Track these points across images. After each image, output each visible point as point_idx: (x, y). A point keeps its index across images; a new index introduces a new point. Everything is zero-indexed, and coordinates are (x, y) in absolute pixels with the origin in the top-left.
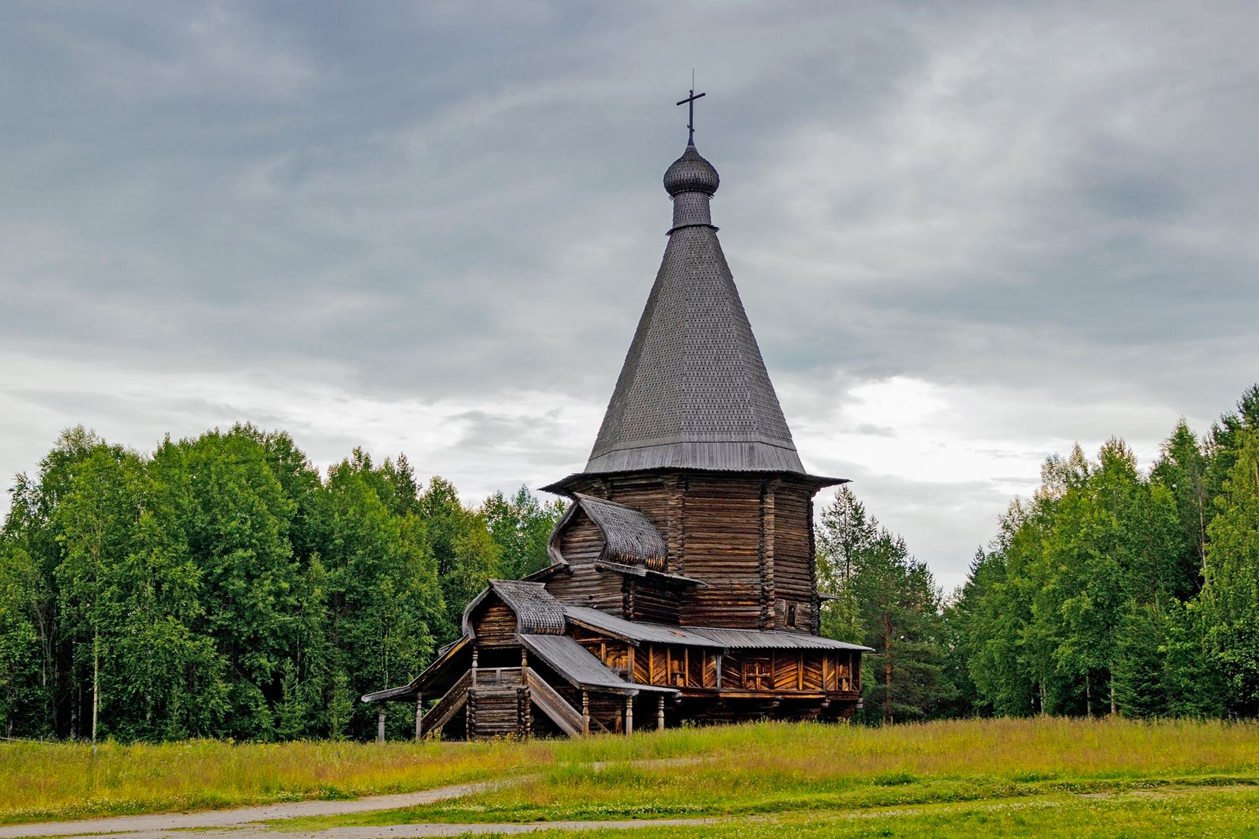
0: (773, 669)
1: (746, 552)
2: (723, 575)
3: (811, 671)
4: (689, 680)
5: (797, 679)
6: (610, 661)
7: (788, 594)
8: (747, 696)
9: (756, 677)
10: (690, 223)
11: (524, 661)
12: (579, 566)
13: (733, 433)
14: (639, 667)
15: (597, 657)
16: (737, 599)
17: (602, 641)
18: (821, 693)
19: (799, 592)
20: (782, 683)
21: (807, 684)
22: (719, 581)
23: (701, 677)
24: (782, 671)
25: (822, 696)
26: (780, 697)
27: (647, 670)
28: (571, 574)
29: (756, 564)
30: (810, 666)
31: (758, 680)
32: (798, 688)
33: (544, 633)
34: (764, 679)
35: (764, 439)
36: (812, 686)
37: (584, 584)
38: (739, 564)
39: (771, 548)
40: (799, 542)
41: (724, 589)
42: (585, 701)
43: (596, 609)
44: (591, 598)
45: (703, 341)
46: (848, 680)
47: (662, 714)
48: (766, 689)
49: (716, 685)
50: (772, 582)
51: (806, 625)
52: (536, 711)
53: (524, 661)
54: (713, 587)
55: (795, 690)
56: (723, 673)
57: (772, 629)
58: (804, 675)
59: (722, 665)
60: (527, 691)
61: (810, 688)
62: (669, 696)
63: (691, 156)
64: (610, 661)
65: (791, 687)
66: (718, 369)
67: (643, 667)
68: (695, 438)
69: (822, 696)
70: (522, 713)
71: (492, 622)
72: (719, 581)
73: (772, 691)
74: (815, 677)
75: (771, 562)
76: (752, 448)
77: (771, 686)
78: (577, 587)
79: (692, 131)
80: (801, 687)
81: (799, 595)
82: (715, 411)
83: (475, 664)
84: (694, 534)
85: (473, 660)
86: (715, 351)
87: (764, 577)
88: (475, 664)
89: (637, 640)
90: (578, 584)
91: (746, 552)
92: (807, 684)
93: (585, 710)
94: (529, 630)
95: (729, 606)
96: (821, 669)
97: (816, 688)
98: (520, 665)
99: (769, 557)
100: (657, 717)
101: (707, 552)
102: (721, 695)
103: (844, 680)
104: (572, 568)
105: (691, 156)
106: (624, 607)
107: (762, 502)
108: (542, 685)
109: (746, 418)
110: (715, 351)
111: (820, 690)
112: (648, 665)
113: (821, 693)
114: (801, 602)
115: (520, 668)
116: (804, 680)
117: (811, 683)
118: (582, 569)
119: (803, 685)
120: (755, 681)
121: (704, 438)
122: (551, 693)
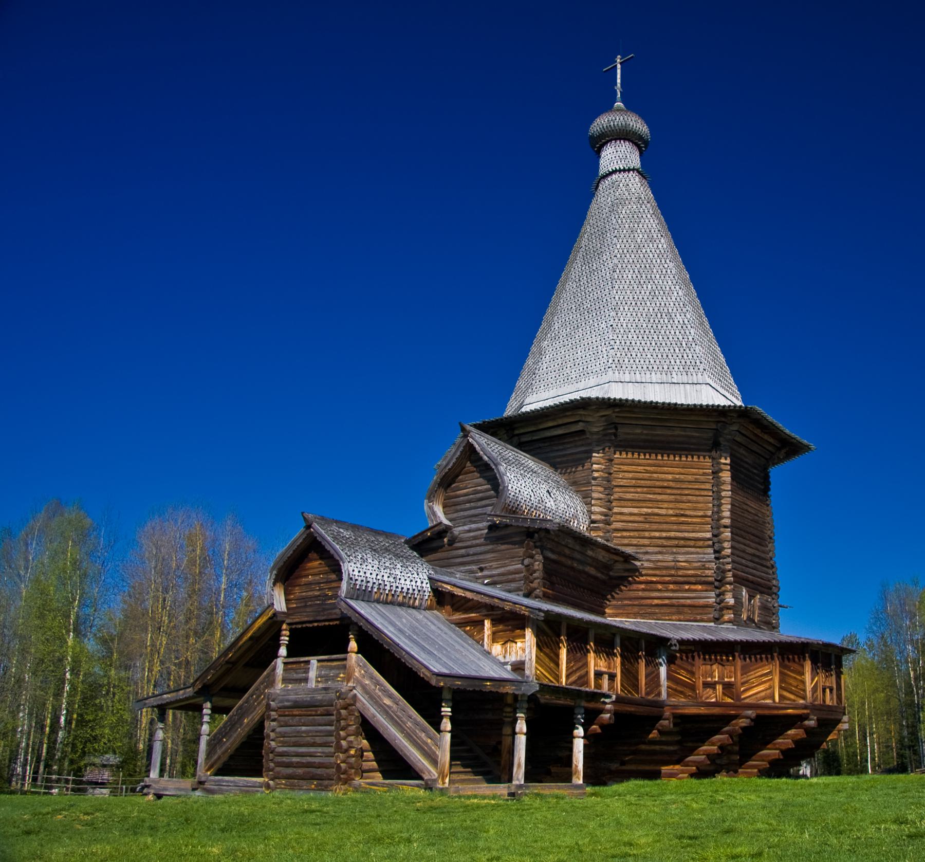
1: (695, 520)
2: (664, 550)
4: (622, 685)
9: (716, 683)
11: (353, 645)
12: (466, 528)
17: (487, 616)
20: (751, 693)
21: (786, 694)
22: (660, 557)
24: (752, 675)
25: (805, 711)
26: (749, 712)
29: (709, 535)
30: (788, 668)
31: (719, 688)
32: (774, 700)
34: (728, 687)
36: (792, 697)
37: (472, 551)
38: (686, 535)
39: (727, 514)
40: (757, 518)
41: (667, 568)
44: (481, 569)
45: (634, 276)
46: (831, 690)
50: (729, 560)
52: (369, 730)
53: (353, 645)
54: (651, 565)
55: (768, 701)
58: (781, 681)
61: (789, 699)
65: (764, 699)
66: (653, 305)
67: (551, 659)
71: (310, 584)
72: (660, 557)
73: (738, 703)
74: (795, 683)
75: (727, 534)
77: (737, 697)
78: (463, 556)
82: (651, 349)
90: (463, 551)
91: (695, 520)
92: (786, 694)
93: (447, 725)
95: (673, 591)
96: (803, 674)
99: (726, 527)
103: (828, 691)
104: (457, 531)
106: (526, 578)
109: (690, 357)
111: (802, 701)
112: (558, 656)
114: (761, 593)
116: (781, 688)
118: (469, 531)
119: (781, 696)
120: (715, 689)
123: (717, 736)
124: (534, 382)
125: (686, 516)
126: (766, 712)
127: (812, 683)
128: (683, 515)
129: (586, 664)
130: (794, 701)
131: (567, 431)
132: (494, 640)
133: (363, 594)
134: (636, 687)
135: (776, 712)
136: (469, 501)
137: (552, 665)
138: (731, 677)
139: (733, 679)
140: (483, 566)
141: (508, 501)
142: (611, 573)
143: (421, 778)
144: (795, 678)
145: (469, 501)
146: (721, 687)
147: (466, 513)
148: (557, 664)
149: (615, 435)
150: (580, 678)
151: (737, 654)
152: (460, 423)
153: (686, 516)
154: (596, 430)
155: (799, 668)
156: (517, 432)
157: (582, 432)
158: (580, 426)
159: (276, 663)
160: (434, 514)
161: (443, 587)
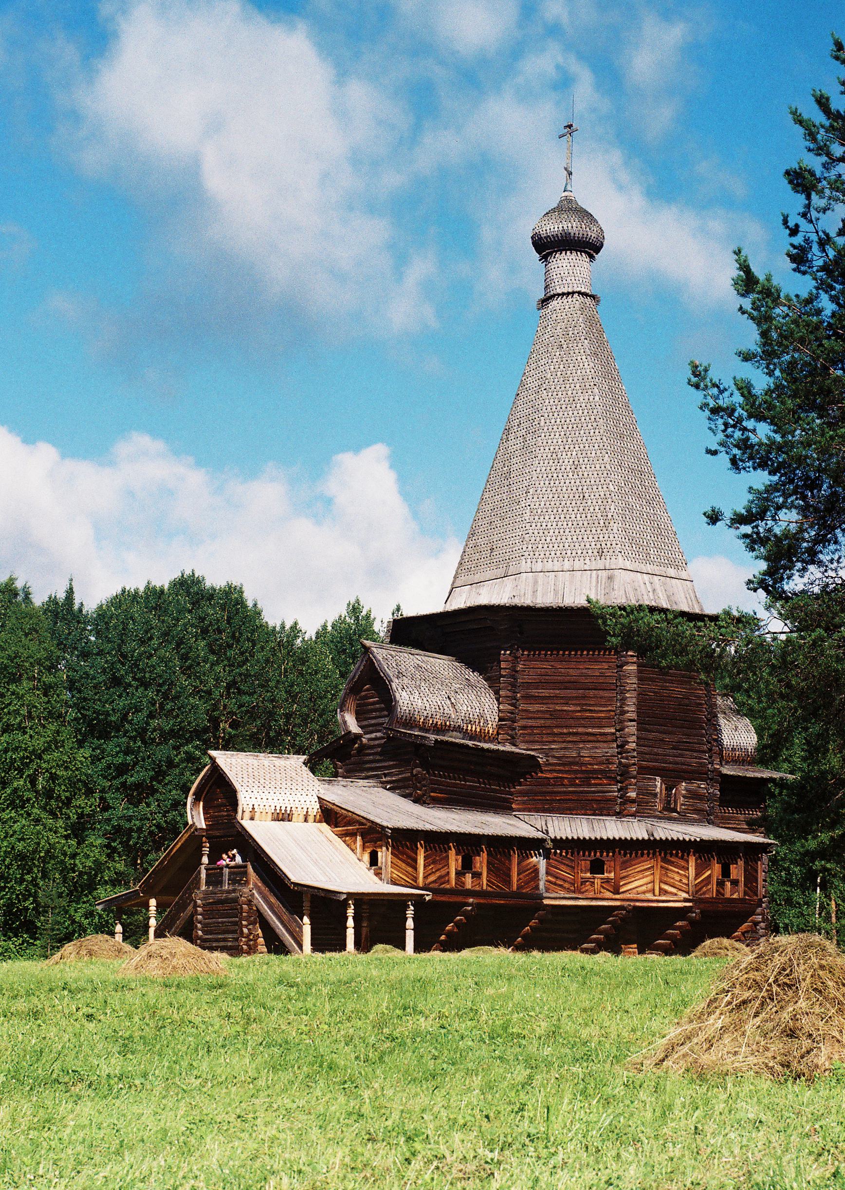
0: (618, 868)
3: (671, 870)
5: (653, 882)
7: (664, 769)
10: (559, 291)
13: (577, 559)
14: (400, 863)
15: (353, 850)
16: (588, 777)
18: (686, 900)
19: (684, 767)
22: (562, 753)
23: (509, 876)
24: (630, 871)
30: (672, 863)
35: (628, 565)
36: (674, 890)
43: (387, 790)
47: (410, 923)
49: (537, 887)
51: (697, 811)
55: (649, 896)
57: (633, 815)
59: (488, 862)
61: (671, 893)
62: (418, 901)
65: (644, 893)
67: (408, 864)
68: (539, 567)
69: (690, 904)
70: (244, 923)
72: (561, 753)
74: (677, 878)
75: (632, 728)
76: (610, 578)
79: (570, 174)
81: (684, 771)
84: (534, 692)
85: (203, 855)
86: (574, 453)
87: (621, 746)
88: (205, 860)
89: (388, 827)
96: (688, 869)
97: (680, 893)
100: (404, 929)
101: (547, 716)
102: (546, 902)
110: (574, 453)
112: (415, 861)
113: (686, 900)
116: (661, 881)
119: (660, 889)
121: (549, 566)
123: (603, 926)
125: (591, 711)
127: (696, 880)
128: (586, 711)
129: (447, 865)
134: (508, 881)
135: (638, 904)
136: (375, 710)
137: (410, 869)
138: (610, 872)
139: (612, 874)
144: (678, 873)
145: (375, 710)
147: (373, 722)
148: (415, 868)
150: (440, 877)
151: (617, 850)
153: (591, 711)
155: (683, 863)
160: (345, 722)
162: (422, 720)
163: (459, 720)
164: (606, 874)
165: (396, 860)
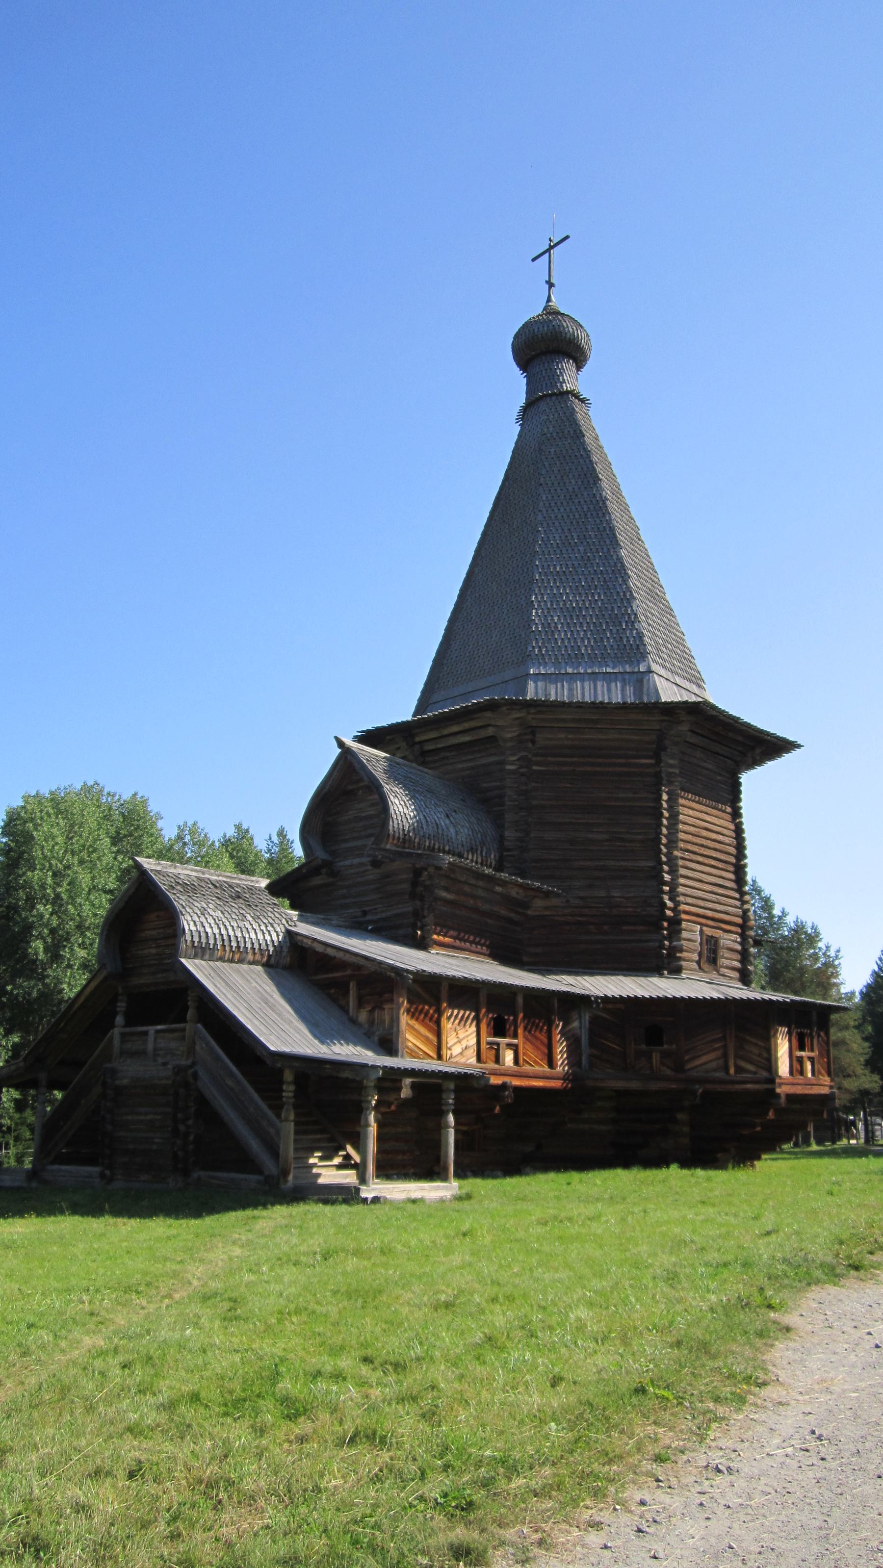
5: (725, 1056)
6: (363, 1016)
8: (635, 1085)
11: (190, 1014)
21: (743, 1064)
27: (439, 1035)
28: (333, 874)
32: (726, 1069)
33: (240, 961)
42: (289, 1091)
44: (365, 913)
47: (451, 1118)
48: (668, 1072)
55: (720, 1075)
56: (592, 1044)
60: (190, 1072)
61: (749, 1072)
63: (550, 311)
64: (363, 1016)
65: (715, 1070)
70: (180, 1115)
74: (757, 1051)
77: (679, 1067)
79: (551, 285)
80: (732, 1071)
83: (119, 1020)
88: (119, 1020)
89: (407, 971)
92: (743, 1064)
94: (202, 951)
98: (184, 1020)
105: (550, 311)
107: (659, 761)
108: (218, 1058)
115: (182, 1025)
116: (737, 1056)
117: (751, 1062)
120: (650, 1058)
122: (231, 1075)
124: (441, 675)
126: (719, 1088)
130: (755, 1073)
131: (476, 737)
132: (360, 1005)
133: (202, 951)
140: (367, 909)
141: (391, 831)
142: (529, 912)
143: (260, 1172)
146: (658, 1055)
149: (533, 742)
152: (337, 739)
154: (509, 735)
156: (417, 739)
157: (492, 739)
158: (490, 731)
159: (113, 1033)
161: (302, 941)
162: (417, 840)
163: (460, 846)
164: (665, 1046)
165: (413, 1022)
